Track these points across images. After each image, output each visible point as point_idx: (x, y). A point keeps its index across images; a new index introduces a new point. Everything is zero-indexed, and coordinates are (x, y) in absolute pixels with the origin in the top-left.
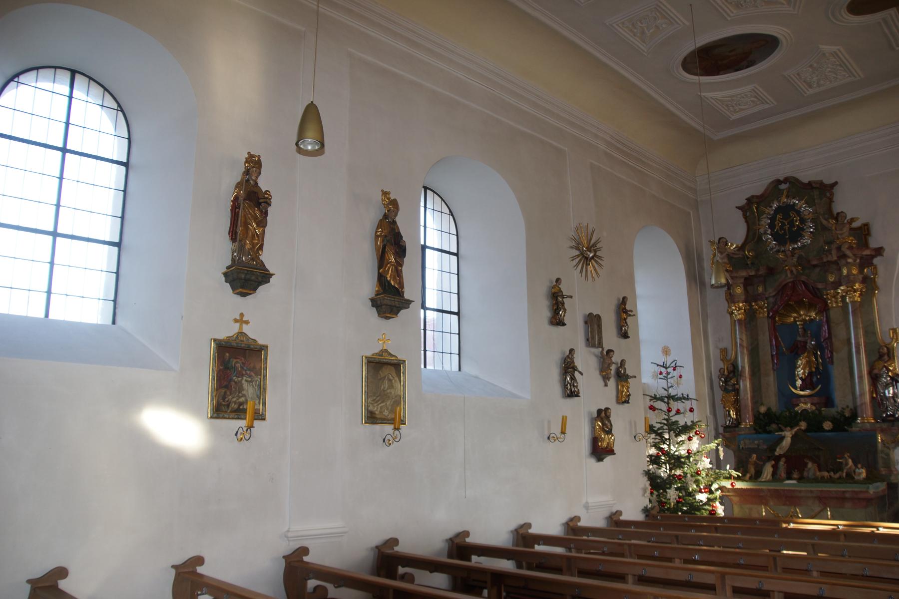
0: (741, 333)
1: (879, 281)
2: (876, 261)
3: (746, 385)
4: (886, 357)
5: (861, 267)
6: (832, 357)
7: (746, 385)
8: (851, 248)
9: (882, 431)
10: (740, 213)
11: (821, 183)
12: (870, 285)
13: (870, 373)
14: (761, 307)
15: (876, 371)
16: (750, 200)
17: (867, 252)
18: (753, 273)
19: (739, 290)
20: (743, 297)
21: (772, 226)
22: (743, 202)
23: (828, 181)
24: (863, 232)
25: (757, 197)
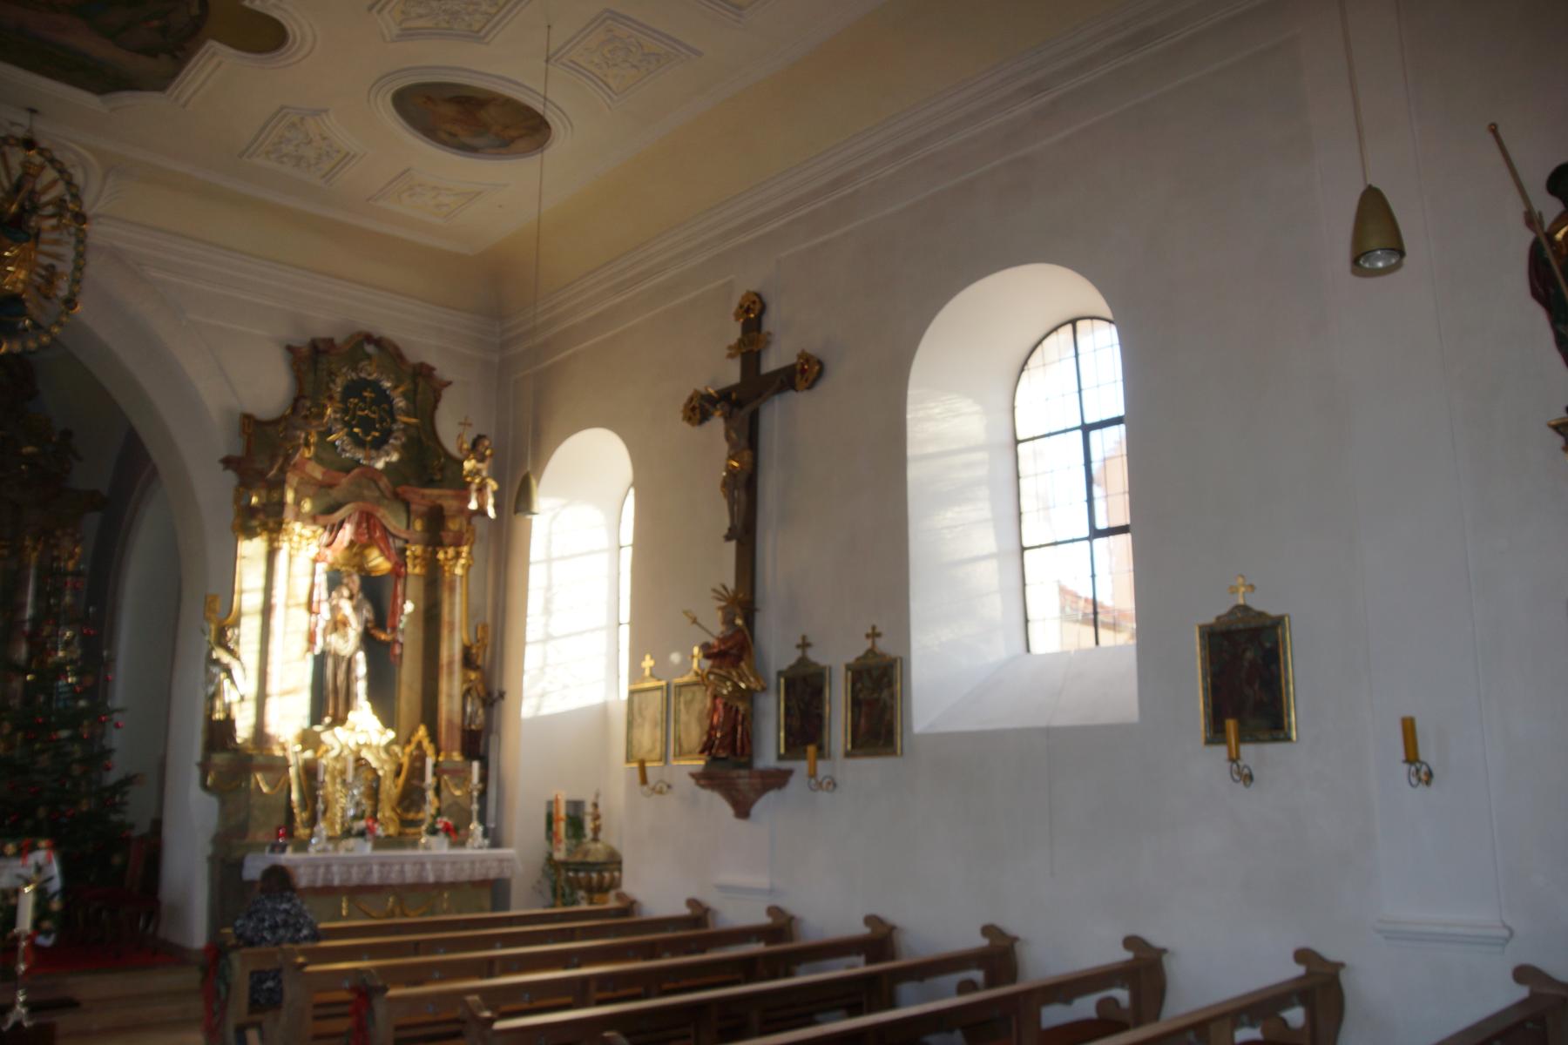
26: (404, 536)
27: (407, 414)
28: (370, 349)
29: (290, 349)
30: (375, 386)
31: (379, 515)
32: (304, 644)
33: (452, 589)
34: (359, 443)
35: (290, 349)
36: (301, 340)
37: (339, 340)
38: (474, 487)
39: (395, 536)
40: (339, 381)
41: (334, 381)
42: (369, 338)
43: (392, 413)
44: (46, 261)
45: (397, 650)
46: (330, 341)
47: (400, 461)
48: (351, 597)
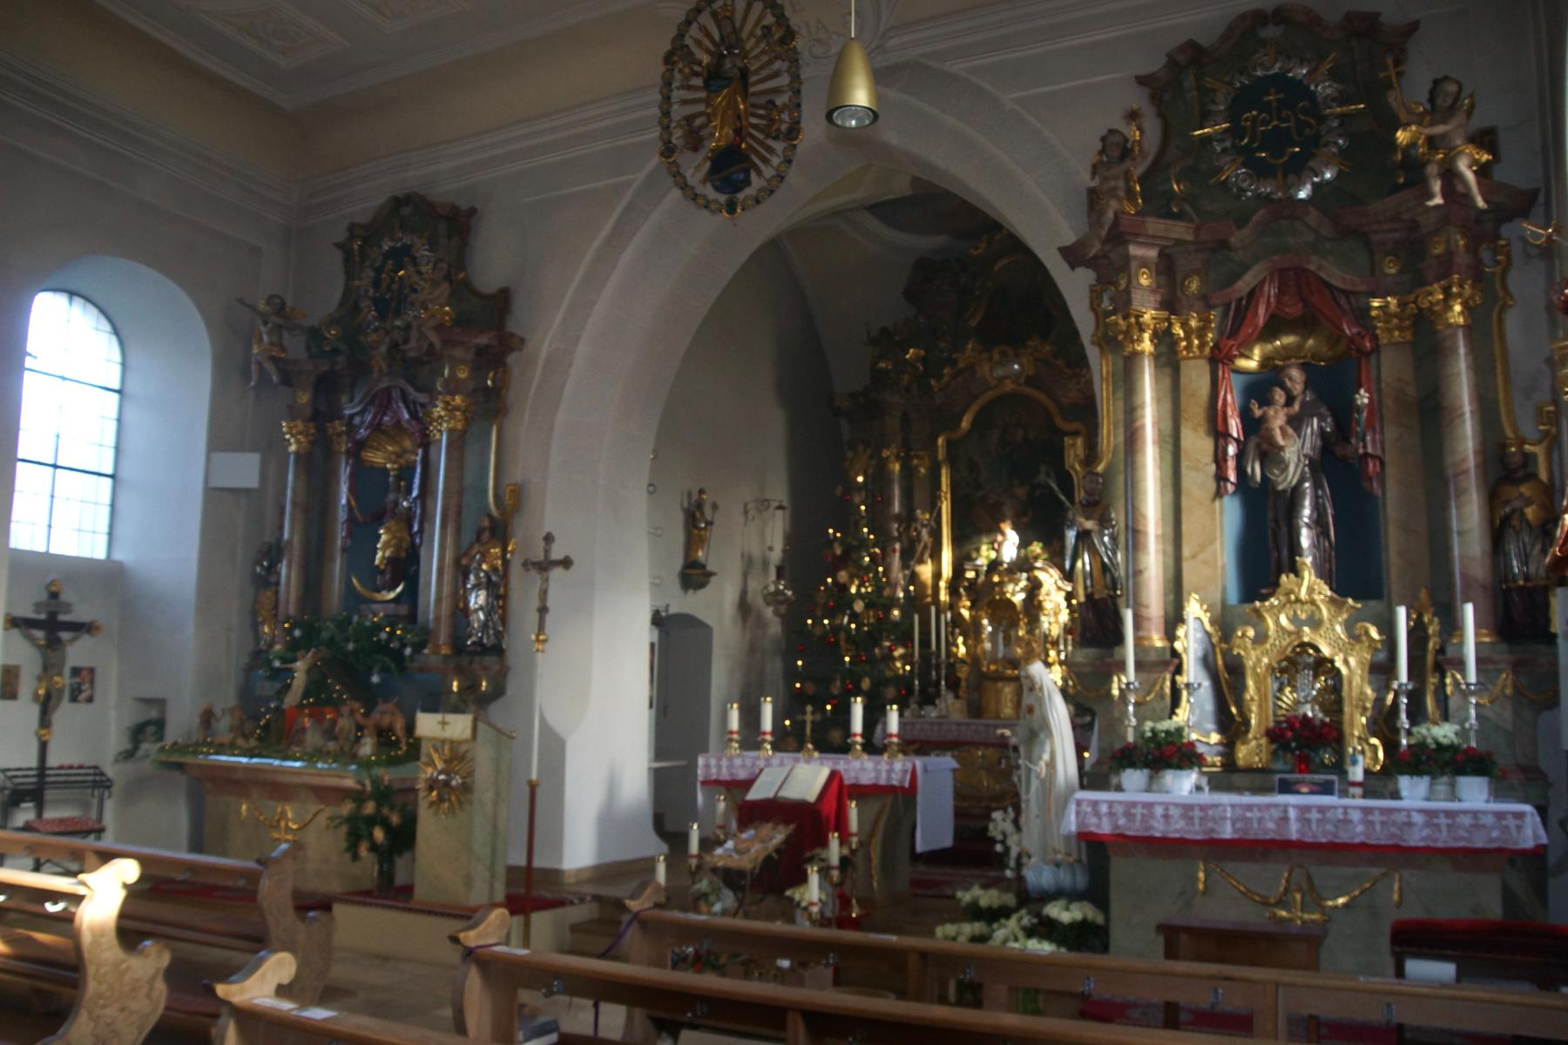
0: (296, 477)
1: (511, 396)
2: (511, 359)
3: (288, 573)
4: (486, 536)
5: (478, 369)
6: (421, 530)
7: (288, 573)
8: (439, 328)
9: (460, 672)
10: (338, 256)
11: (455, 210)
12: (489, 405)
13: (457, 562)
14: (339, 435)
15: (464, 562)
16: (352, 228)
17: (483, 340)
18: (326, 368)
19: (304, 398)
20: (308, 412)
21: (376, 284)
22: (341, 235)
23: (464, 204)
24: (502, 301)
25: (363, 227)
26: (1362, 288)
27: (1344, 99)
28: (1271, 32)
29: (1142, 81)
30: (1280, 81)
31: (1312, 267)
32: (1212, 486)
33: (1455, 350)
34: (1261, 171)
35: (1142, 81)
36: (1153, 63)
37: (1205, 40)
38: (1432, 170)
39: (1346, 293)
40: (1220, 97)
41: (1213, 102)
42: (1258, 18)
43: (1314, 107)
44: (762, 100)
45: (1371, 466)
46: (1192, 46)
47: (1340, 173)
48: (1290, 401)
